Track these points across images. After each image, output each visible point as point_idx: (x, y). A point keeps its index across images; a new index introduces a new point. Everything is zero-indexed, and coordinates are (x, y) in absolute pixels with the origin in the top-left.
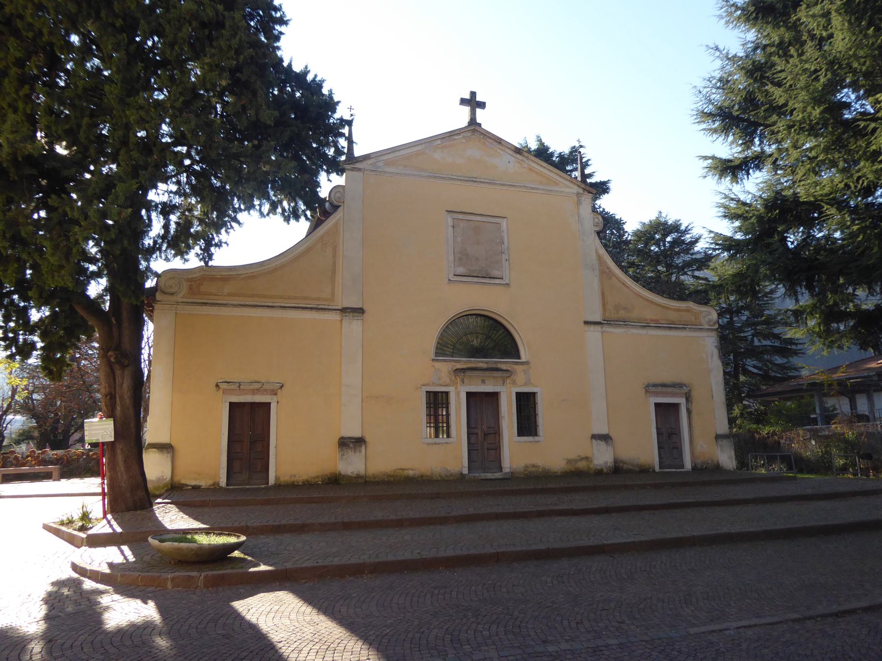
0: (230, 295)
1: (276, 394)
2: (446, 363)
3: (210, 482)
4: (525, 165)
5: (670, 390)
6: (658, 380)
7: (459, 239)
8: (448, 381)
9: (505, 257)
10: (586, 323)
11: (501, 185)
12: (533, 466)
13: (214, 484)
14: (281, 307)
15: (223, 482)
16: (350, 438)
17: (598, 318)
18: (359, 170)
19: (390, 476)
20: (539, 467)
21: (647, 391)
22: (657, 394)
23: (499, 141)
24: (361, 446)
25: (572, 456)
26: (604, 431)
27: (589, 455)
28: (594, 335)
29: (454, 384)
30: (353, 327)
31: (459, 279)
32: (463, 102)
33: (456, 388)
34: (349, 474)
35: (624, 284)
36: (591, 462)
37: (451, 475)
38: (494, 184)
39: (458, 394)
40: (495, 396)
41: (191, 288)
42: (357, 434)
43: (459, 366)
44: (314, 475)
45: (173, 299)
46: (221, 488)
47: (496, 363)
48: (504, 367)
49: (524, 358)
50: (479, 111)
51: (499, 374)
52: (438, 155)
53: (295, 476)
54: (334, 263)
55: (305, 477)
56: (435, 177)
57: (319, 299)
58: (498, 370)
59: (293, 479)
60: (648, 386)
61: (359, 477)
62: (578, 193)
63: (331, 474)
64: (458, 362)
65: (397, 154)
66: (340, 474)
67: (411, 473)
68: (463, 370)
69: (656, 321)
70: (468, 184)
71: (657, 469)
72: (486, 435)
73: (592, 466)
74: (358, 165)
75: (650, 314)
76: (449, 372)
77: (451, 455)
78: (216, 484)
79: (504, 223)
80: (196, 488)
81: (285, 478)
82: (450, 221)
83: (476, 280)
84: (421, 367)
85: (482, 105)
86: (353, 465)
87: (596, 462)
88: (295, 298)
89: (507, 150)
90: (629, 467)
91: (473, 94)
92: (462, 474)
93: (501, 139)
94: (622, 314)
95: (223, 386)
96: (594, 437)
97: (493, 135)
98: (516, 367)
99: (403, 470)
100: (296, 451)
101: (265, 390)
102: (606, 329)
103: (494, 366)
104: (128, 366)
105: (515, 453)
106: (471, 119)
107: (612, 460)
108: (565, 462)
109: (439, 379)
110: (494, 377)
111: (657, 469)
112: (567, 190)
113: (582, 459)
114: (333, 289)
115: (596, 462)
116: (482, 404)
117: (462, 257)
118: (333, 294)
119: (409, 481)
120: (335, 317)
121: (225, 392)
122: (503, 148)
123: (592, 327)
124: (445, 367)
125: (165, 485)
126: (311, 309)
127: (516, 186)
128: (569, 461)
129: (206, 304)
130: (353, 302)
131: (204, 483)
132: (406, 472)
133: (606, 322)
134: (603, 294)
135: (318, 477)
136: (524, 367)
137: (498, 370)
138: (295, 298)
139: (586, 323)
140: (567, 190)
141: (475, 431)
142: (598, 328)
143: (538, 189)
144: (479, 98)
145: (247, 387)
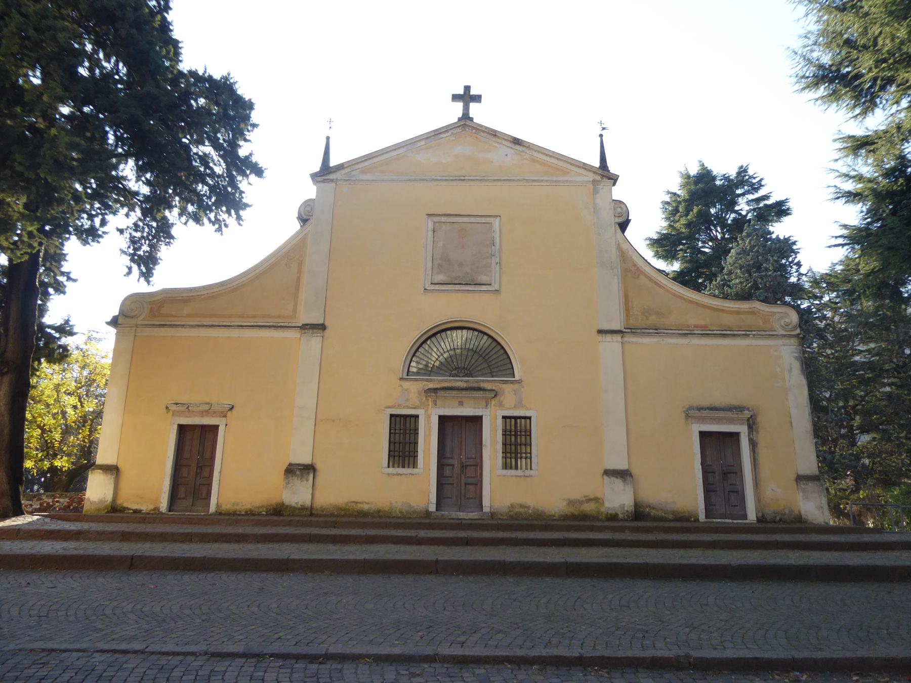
0: (189, 316)
1: (225, 416)
2: (415, 383)
3: (151, 507)
4: (527, 156)
5: (721, 414)
6: (706, 403)
7: (440, 244)
8: (417, 402)
9: (495, 260)
10: (600, 332)
11: (494, 180)
12: (522, 506)
13: (154, 509)
14: (239, 326)
15: (164, 506)
16: (299, 465)
17: (617, 326)
18: (332, 181)
19: (341, 509)
20: (528, 507)
21: (688, 417)
22: (703, 420)
23: (494, 134)
24: (308, 474)
25: (576, 495)
26: (622, 465)
27: (599, 496)
28: (612, 345)
29: (423, 405)
30: (313, 343)
31: (437, 287)
32: (455, 98)
33: (426, 411)
34: (294, 505)
35: (657, 284)
36: (603, 504)
37: (415, 512)
38: (487, 180)
39: (428, 417)
40: (478, 420)
41: (152, 310)
42: (307, 460)
43: (431, 386)
44: (257, 504)
45: (134, 321)
46: (162, 513)
47: (477, 382)
48: (488, 386)
49: (517, 378)
50: (473, 106)
51: (480, 394)
52: (421, 157)
53: (238, 504)
54: (299, 279)
55: (249, 507)
56: (415, 180)
57: (279, 317)
58: (480, 389)
59: (236, 507)
60: (691, 408)
61: (303, 508)
62: (594, 181)
63: (277, 504)
64: (431, 381)
65: (375, 160)
66: (283, 504)
67: (366, 507)
68: (435, 390)
69: (704, 327)
70: (454, 183)
71: (702, 517)
72: (464, 467)
73: (603, 510)
74: (331, 177)
75: (692, 320)
76: (419, 393)
77: (416, 488)
78: (156, 509)
79: (496, 223)
80: (136, 511)
81: (227, 507)
82: (431, 226)
83: (457, 287)
84: (383, 385)
85: (477, 99)
86: (299, 495)
87: (607, 504)
88: (254, 317)
89: (504, 142)
90: (660, 513)
91: (467, 88)
92: (427, 511)
93: (496, 131)
94: (654, 319)
95: (173, 408)
96: (608, 473)
97: (486, 128)
98: (504, 386)
99: (357, 503)
100: (242, 479)
101: (215, 412)
102: (629, 338)
103: (475, 385)
104: (7, 373)
105: (501, 489)
106: (463, 115)
107: (632, 503)
108: (565, 503)
109: (407, 400)
110: (475, 398)
111: (702, 517)
112: (579, 179)
113: (589, 500)
114: (295, 306)
115: (607, 504)
116: (459, 431)
117: (442, 263)
118: (295, 311)
119: (363, 514)
120: (294, 334)
121: (175, 413)
122: (499, 141)
123: (609, 338)
124: (414, 388)
125: (106, 508)
126: (270, 327)
127: (513, 180)
128: (571, 502)
129: (163, 326)
130: (314, 318)
131: (145, 507)
132: (359, 506)
133: (629, 330)
134: (626, 297)
135: (262, 507)
136: (516, 386)
137: (480, 389)
138: (254, 317)
139: (600, 332)
140: (579, 179)
141: (451, 462)
142: (617, 338)
143: (542, 181)
144: (473, 92)
145: (195, 409)
